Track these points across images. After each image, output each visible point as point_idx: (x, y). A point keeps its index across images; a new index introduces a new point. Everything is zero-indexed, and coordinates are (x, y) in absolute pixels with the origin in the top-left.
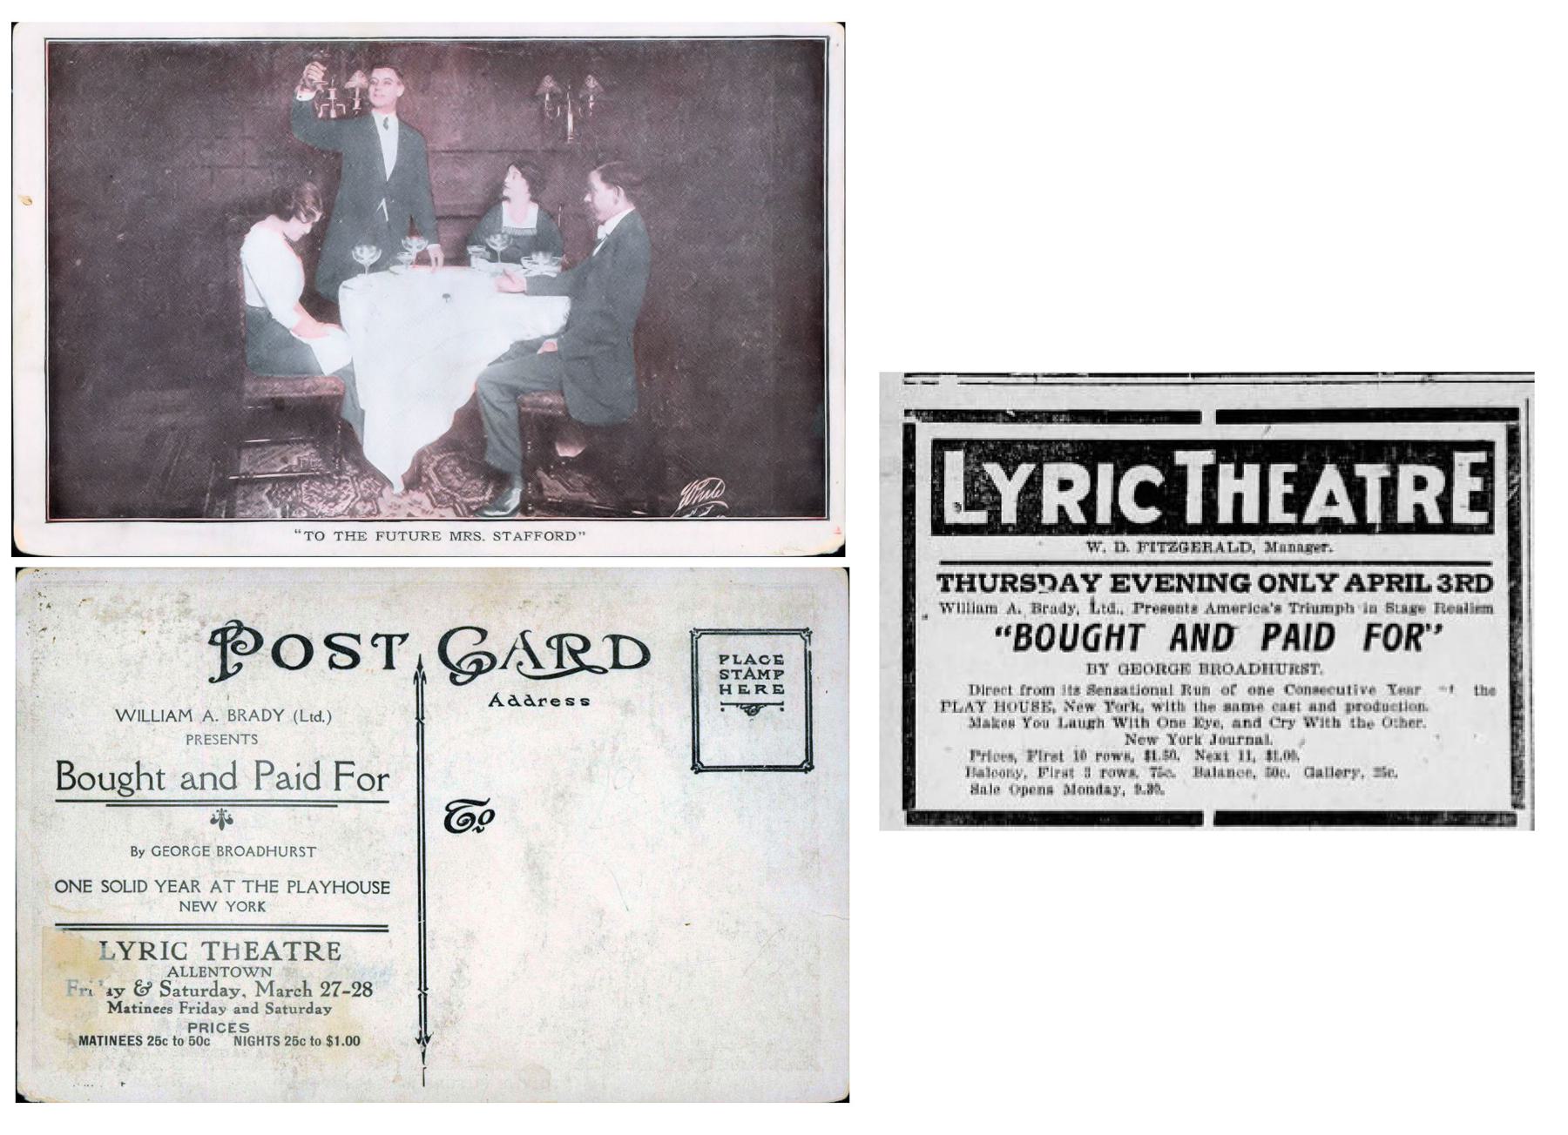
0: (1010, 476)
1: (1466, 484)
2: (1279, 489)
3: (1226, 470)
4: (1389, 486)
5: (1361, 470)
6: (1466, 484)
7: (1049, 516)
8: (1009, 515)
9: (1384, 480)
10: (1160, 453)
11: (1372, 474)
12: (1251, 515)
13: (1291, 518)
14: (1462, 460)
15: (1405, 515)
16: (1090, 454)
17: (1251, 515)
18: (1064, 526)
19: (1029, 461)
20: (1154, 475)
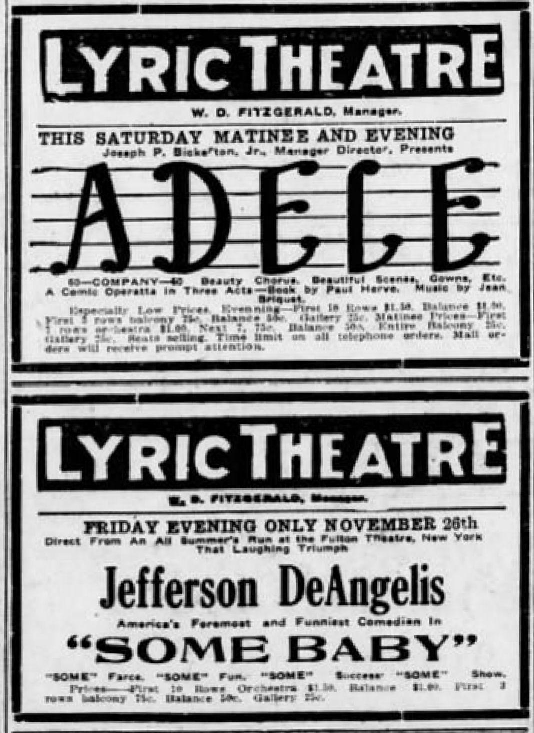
1: (482, 447)
3: (286, 440)
4: (420, 452)
5: (396, 438)
6: (482, 447)
7: (135, 474)
9: (416, 446)
11: (406, 441)
12: (306, 472)
13: (339, 475)
16: (168, 429)
17: (306, 472)
18: (147, 482)
19: (117, 433)
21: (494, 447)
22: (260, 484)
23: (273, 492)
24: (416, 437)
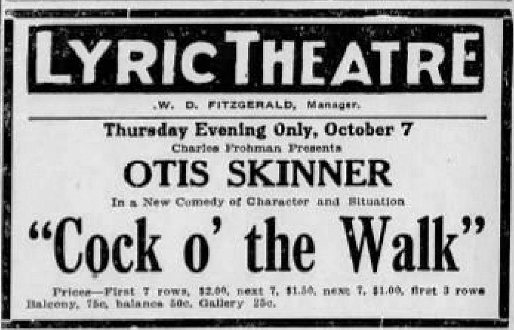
0: (90, 49)
2: (310, 59)
3: (269, 46)
4: (399, 61)
5: (376, 46)
7: (123, 78)
8: (89, 77)
9: (394, 54)
10: (215, 34)
11: (386, 49)
12: (288, 78)
13: (321, 81)
14: (459, 40)
15: (413, 77)
17: (288, 78)
18: (135, 86)
19: (105, 37)
20: (209, 49)
24: (396, 46)
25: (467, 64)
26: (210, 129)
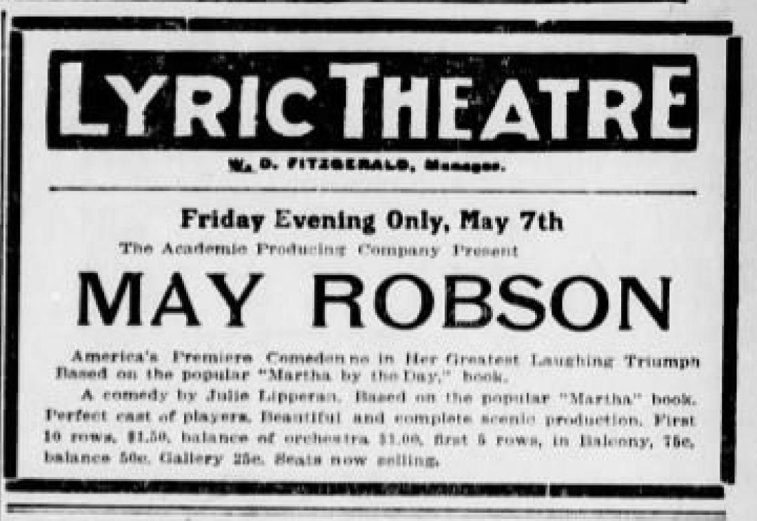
0: (137, 86)
1: (664, 99)
2: (450, 103)
3: (392, 84)
4: (578, 105)
5: (545, 85)
7: (183, 128)
8: (136, 126)
9: (570, 96)
10: (312, 65)
11: (559, 89)
12: (418, 129)
13: (466, 134)
14: (662, 77)
15: (596, 130)
16: (231, 67)
17: (418, 129)
18: (199, 140)
20: (306, 89)
21: (680, 99)
22: (353, 145)
23: (371, 156)
24: (573, 85)
25: (674, 109)
26: (296, 218)
